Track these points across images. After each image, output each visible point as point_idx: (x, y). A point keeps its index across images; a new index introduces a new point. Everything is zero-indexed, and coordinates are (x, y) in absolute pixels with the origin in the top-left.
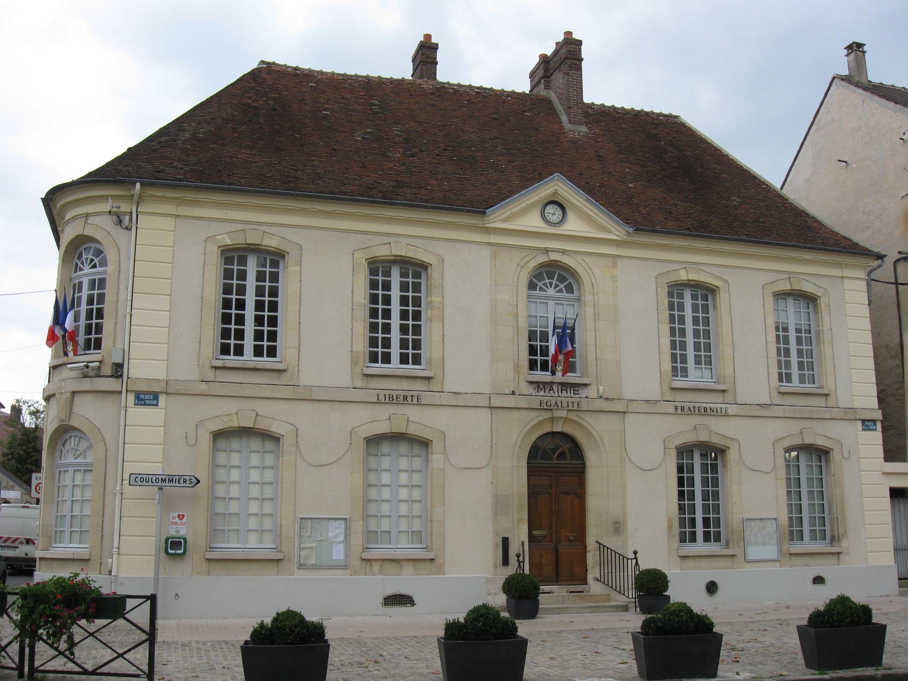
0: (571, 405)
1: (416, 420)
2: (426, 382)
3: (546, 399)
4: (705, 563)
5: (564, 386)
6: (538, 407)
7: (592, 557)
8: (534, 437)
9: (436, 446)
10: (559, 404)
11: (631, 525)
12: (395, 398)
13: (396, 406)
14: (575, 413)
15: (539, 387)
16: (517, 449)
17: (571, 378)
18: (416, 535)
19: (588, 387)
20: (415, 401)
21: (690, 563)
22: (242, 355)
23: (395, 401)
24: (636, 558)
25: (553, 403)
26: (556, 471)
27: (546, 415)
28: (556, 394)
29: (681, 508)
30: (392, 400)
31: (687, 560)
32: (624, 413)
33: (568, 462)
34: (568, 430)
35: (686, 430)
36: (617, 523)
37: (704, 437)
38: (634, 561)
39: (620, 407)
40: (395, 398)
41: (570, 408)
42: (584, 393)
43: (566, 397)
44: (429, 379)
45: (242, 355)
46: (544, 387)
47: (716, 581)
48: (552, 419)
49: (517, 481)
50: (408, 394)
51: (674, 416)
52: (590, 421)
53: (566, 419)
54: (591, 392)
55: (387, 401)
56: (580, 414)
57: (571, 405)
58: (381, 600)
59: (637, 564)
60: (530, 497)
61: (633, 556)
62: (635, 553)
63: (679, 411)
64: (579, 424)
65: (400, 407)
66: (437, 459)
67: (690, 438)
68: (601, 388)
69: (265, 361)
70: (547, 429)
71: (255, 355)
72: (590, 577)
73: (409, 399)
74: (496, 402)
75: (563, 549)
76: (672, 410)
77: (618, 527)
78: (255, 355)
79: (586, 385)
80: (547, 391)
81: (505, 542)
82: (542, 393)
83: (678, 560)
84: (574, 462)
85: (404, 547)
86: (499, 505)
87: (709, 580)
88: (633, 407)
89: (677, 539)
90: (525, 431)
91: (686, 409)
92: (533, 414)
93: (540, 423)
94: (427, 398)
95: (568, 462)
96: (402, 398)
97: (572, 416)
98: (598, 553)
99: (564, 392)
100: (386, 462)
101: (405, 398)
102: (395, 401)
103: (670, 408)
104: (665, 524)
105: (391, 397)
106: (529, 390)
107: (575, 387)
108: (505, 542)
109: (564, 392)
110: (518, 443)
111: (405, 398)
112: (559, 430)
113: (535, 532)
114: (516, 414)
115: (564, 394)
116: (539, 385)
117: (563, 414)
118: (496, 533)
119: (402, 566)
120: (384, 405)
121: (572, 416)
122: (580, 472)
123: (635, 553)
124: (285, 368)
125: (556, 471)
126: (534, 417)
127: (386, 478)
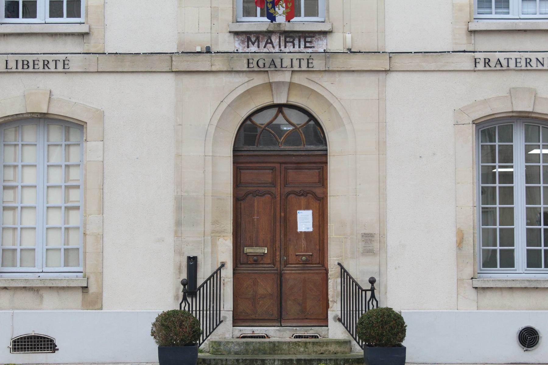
0: (296, 63)
1: (65, 94)
2: (78, 40)
3: (257, 57)
4: (521, 299)
5: (290, 36)
6: (245, 68)
7: (334, 286)
8: (244, 113)
9: (91, 129)
10: (278, 64)
11: (392, 239)
12: (31, 64)
13: (33, 76)
14: (306, 75)
15: (249, 39)
16: (212, 130)
17: (302, 22)
18: (69, 254)
19: (329, 37)
20: (60, 68)
21: (490, 298)
22: (35, 16)
23: (31, 69)
24: (372, 290)
25: (268, 62)
26: (279, 162)
27: (258, 80)
28: (277, 49)
29: (487, 215)
30: (25, 66)
31: (489, 295)
32: (386, 71)
33: (301, 147)
34: (295, 100)
35: (494, 95)
36: (368, 237)
37: (523, 105)
38: (369, 294)
39: (382, 63)
40: (31, 64)
41: (296, 68)
42: (321, 45)
43: (292, 51)
44: (83, 35)
45: (35, 16)
46: (258, 39)
47: (537, 328)
48: (270, 85)
49: (220, 174)
50: (50, 58)
51: (474, 75)
52: (327, 86)
53: (291, 86)
54: (334, 43)
55: (20, 69)
56: (313, 76)
57: (296, 63)
58: (8, 343)
59: (373, 296)
60: (238, 199)
61: (369, 287)
62: (372, 281)
63: (480, 66)
64: (312, 91)
65: (40, 77)
66: (93, 147)
67: (501, 107)
68: (349, 36)
69: (65, 23)
70: (264, 100)
71: (51, 16)
72: (331, 315)
73: (52, 65)
74: (181, 64)
75: (292, 274)
76: (470, 65)
77: (371, 242)
78: (51, 16)
79: (325, 33)
80: (262, 44)
81: (192, 263)
82: (253, 48)
83: (473, 294)
84: (312, 147)
85: (55, 270)
86: (184, 210)
87: (524, 325)
88: (399, 62)
89: (480, 259)
90: (225, 105)
91: (492, 64)
92: (243, 78)
93: (249, 93)
94: (75, 64)
95: (301, 147)
96: (41, 64)
97: (299, 79)
98: (339, 280)
99: (290, 45)
100: (30, 155)
101: (46, 64)
102: (31, 69)
103: (466, 62)
104: (453, 239)
105: (25, 64)
106: (236, 45)
107: (307, 36)
108: (192, 263)
109: (290, 45)
110: (215, 122)
111: (46, 64)
112: (283, 101)
113: (248, 250)
114: (211, 80)
115: (289, 48)
116: (248, 37)
117: (286, 77)
118: (179, 252)
119: (42, 297)
120: (17, 76)
121: (299, 79)
122: (319, 163)
123: (372, 281)
124: (87, 30)
125: (279, 162)
126: (239, 84)
127: (30, 177)
